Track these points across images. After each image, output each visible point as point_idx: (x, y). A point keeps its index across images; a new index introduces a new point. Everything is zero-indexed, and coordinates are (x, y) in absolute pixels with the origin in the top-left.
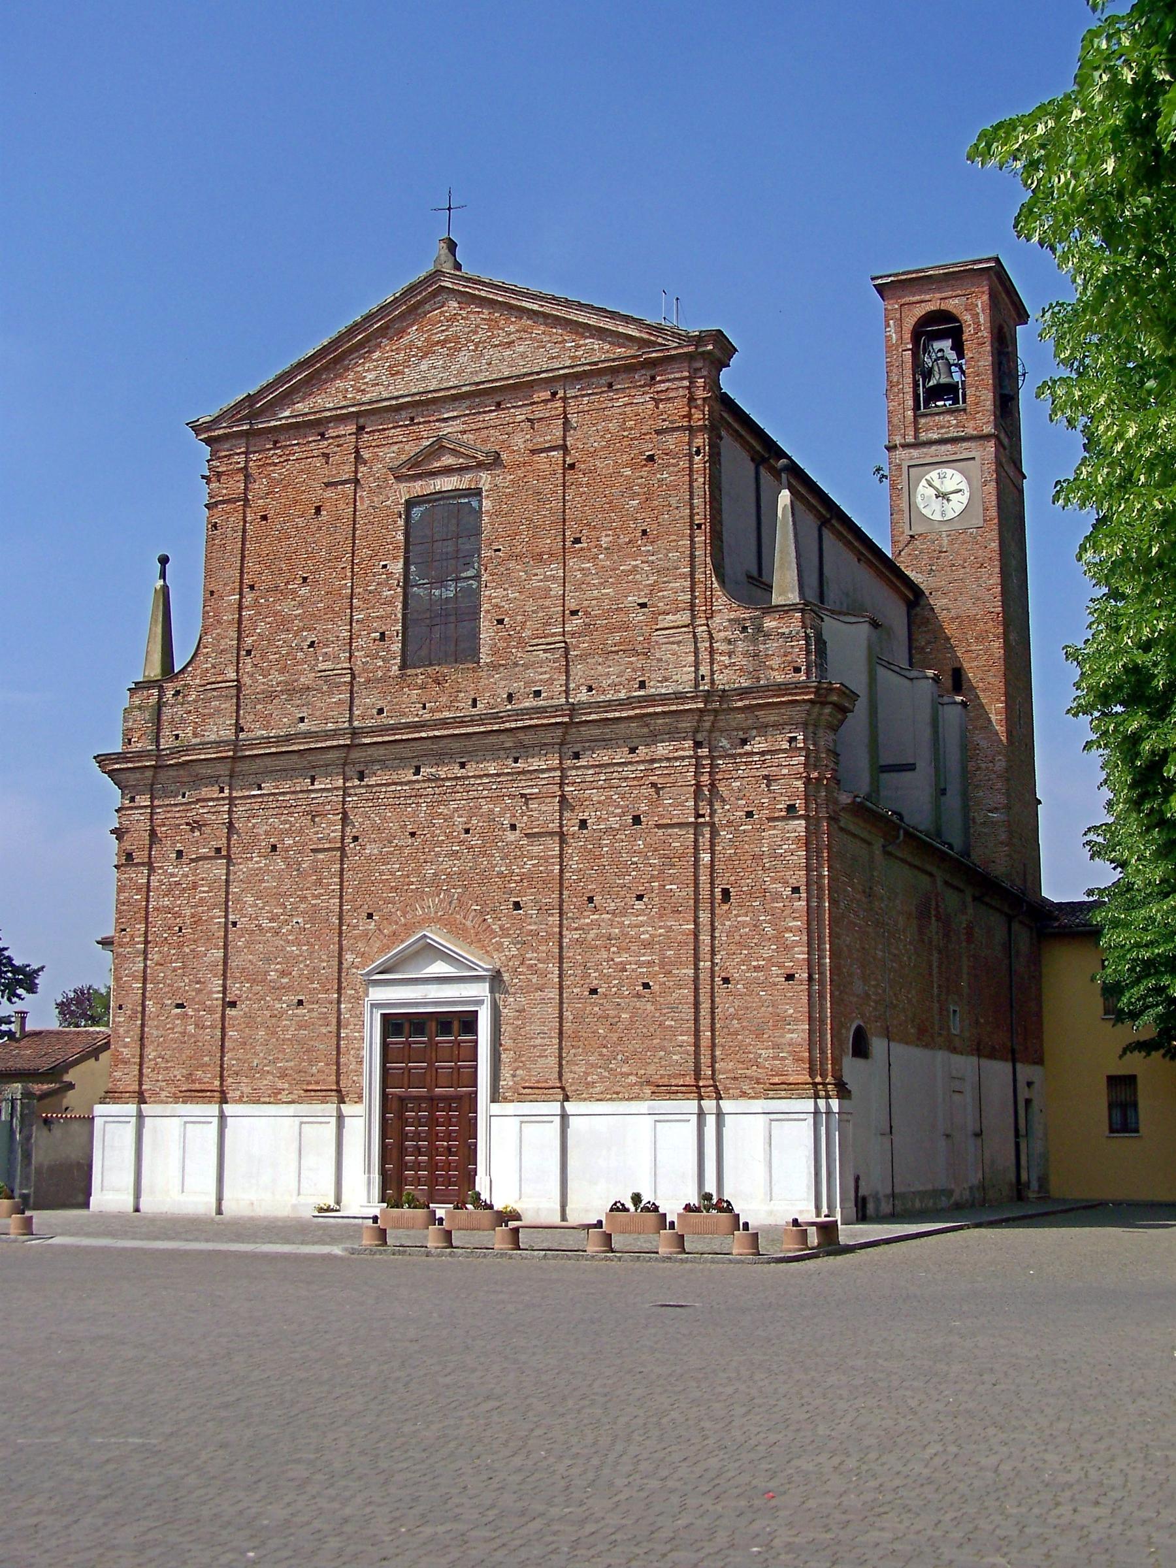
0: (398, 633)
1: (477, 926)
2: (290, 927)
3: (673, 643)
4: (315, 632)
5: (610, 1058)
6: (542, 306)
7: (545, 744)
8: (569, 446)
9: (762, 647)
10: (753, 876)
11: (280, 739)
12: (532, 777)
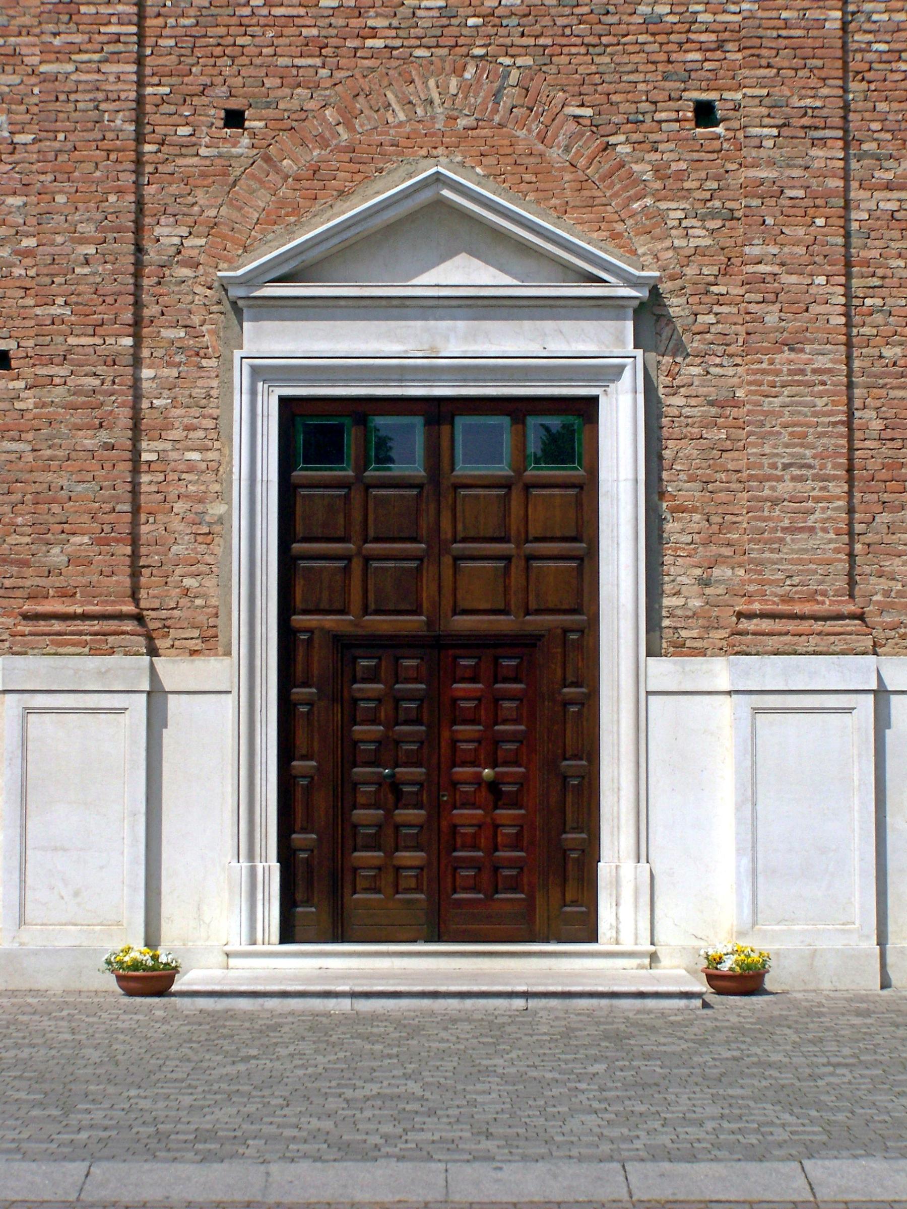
1: (582, 162)
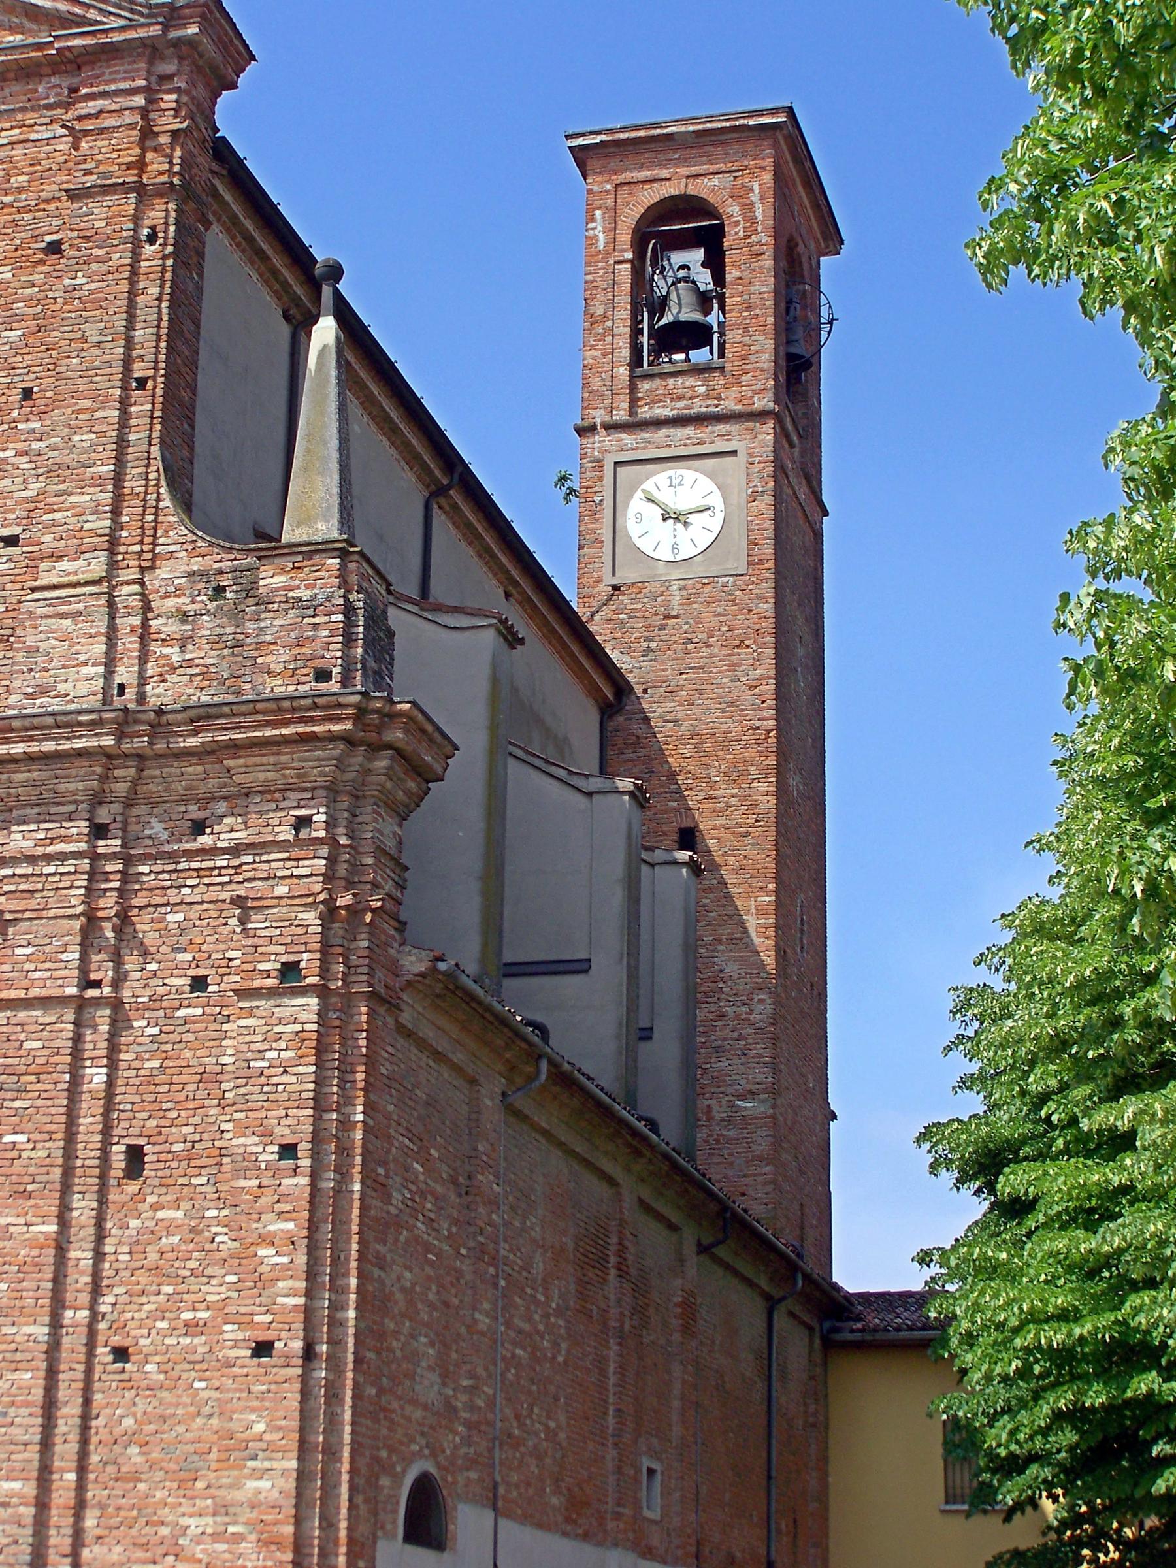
10: (197, 1120)
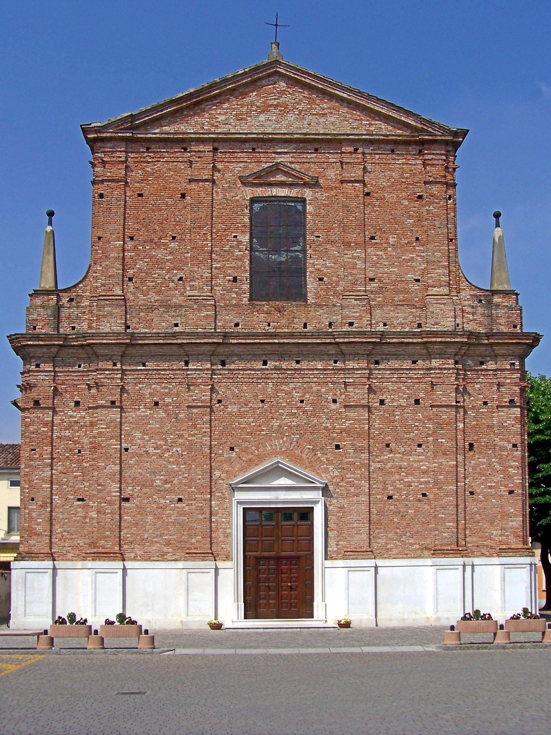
0: (247, 279)
1: (310, 458)
2: (171, 453)
3: (440, 304)
4: (183, 271)
5: (402, 535)
6: (350, 96)
7: (358, 354)
8: (366, 181)
9: (494, 312)
10: (488, 437)
11: (167, 335)
12: (350, 372)
